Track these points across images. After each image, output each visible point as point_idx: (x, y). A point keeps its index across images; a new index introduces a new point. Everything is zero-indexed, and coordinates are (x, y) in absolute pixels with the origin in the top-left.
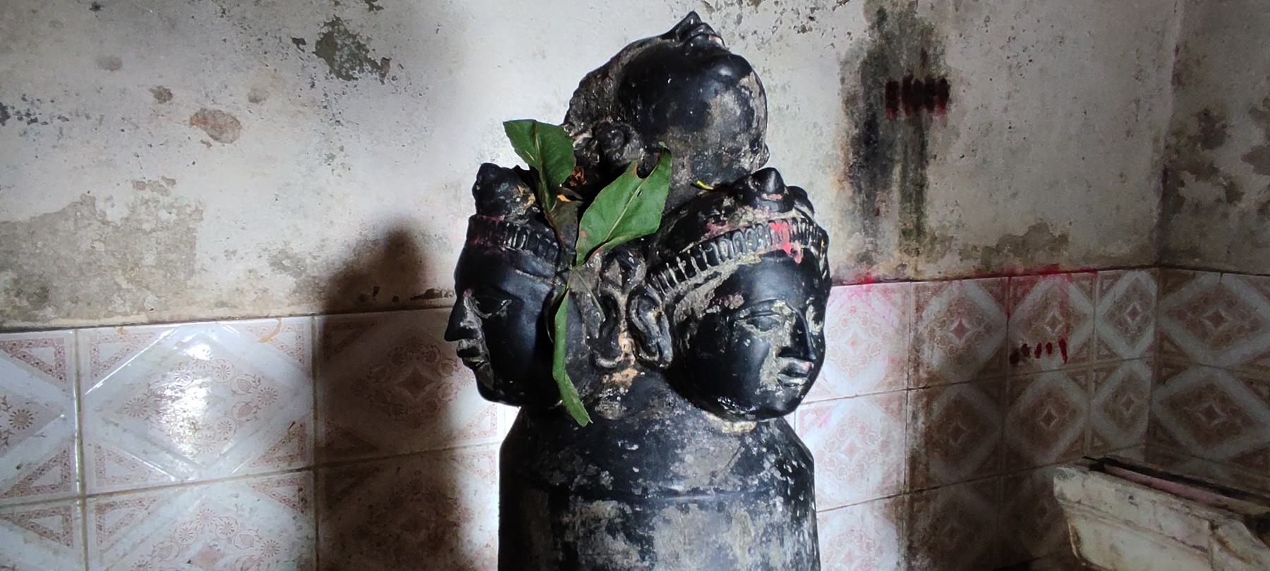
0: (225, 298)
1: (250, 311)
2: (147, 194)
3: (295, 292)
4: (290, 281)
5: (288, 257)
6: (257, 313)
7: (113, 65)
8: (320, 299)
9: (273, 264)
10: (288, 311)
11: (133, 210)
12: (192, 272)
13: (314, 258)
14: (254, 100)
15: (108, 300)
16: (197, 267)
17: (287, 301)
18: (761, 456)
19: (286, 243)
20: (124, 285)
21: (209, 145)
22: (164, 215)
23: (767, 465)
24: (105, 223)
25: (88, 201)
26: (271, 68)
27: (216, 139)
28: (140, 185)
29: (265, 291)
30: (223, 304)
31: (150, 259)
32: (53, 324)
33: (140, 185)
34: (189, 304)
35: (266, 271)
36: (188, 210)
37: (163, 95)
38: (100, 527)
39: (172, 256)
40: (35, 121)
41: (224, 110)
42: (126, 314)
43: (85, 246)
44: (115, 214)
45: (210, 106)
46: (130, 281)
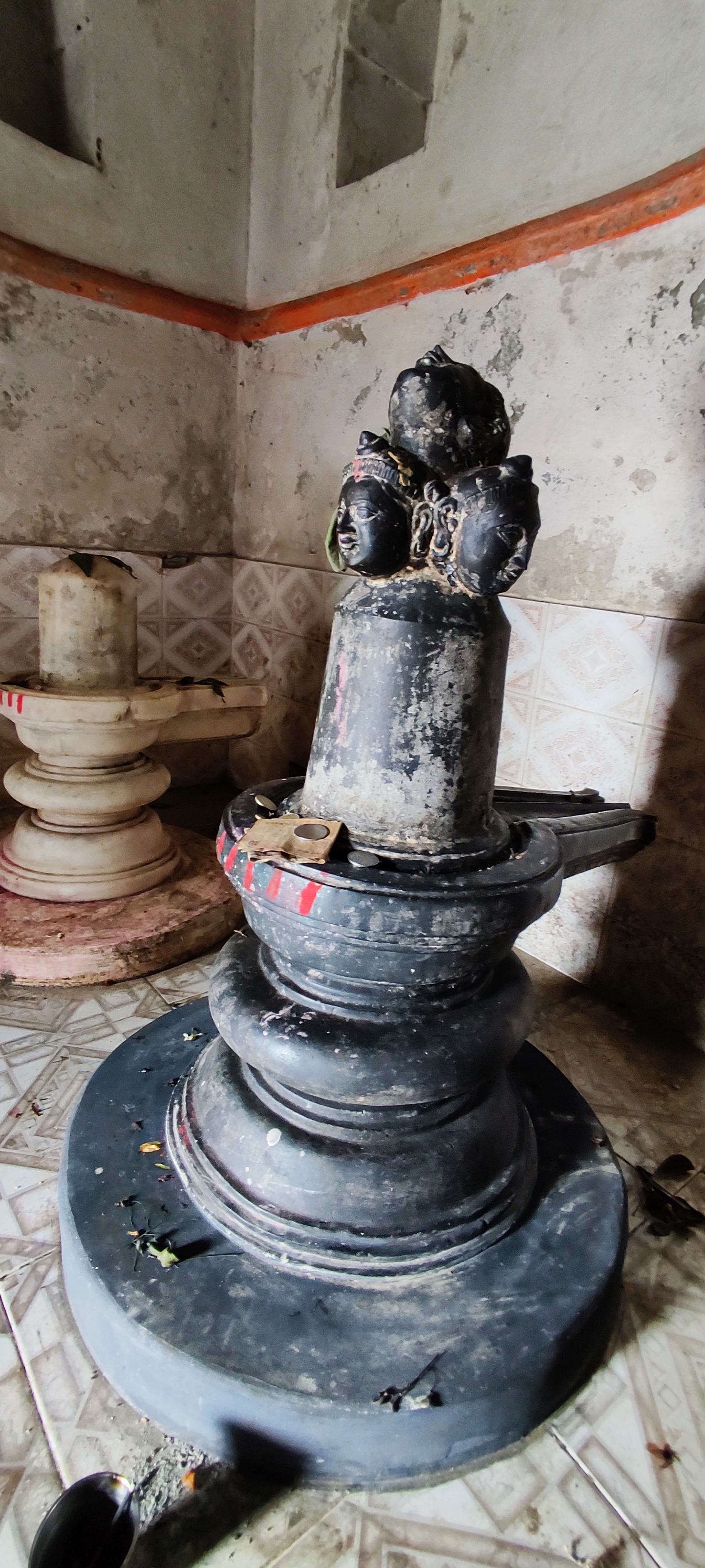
0: (623, 599)
1: (634, 610)
2: (598, 526)
3: (663, 600)
4: (661, 592)
5: (664, 575)
6: (637, 612)
7: (598, 445)
8: (678, 609)
9: (654, 579)
10: (656, 614)
11: (590, 536)
12: (610, 579)
13: (681, 578)
14: (668, 460)
15: (568, 591)
16: (613, 575)
17: (657, 607)
18: (376, 601)
19: (665, 565)
20: (577, 582)
21: (635, 493)
22: (603, 540)
23: (374, 605)
24: (576, 543)
25: (572, 529)
26: (683, 435)
27: (640, 489)
28: (596, 521)
29: (646, 597)
30: (621, 602)
31: (591, 568)
32: (528, 597)
33: (596, 521)
34: (605, 599)
35: (649, 582)
36: (616, 538)
37: (619, 461)
38: (537, 718)
39: (602, 567)
40: (559, 482)
41: (649, 469)
42: (575, 600)
43: (565, 556)
44: (582, 538)
45: (642, 467)
46: (580, 580)
